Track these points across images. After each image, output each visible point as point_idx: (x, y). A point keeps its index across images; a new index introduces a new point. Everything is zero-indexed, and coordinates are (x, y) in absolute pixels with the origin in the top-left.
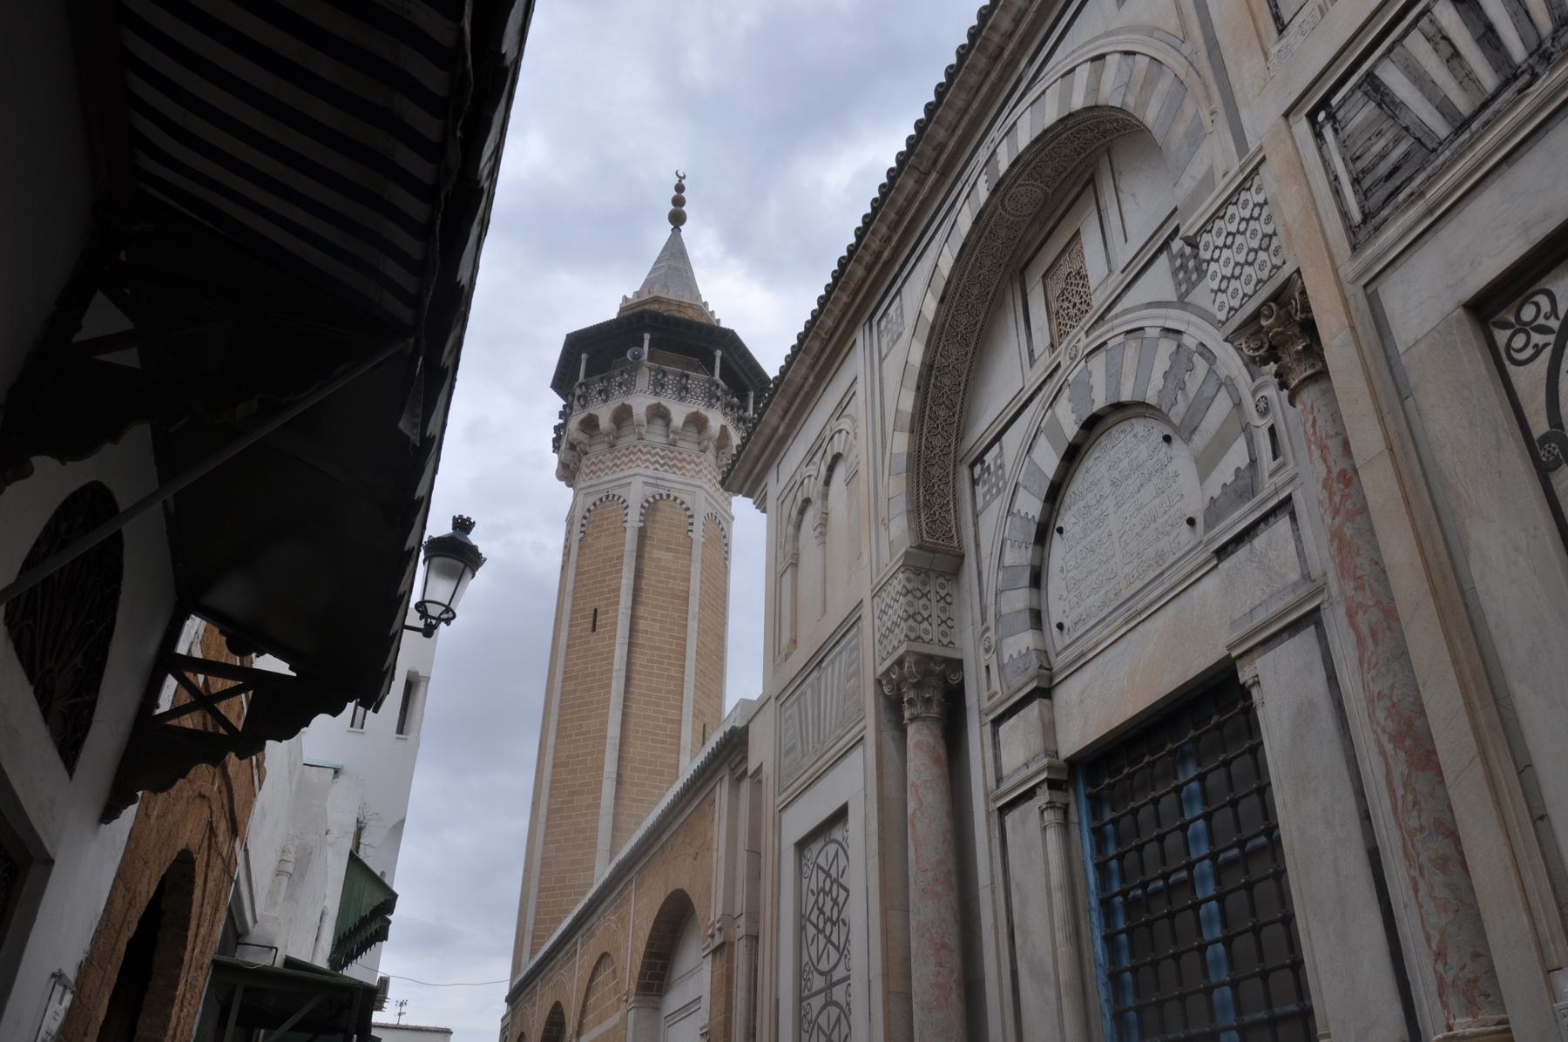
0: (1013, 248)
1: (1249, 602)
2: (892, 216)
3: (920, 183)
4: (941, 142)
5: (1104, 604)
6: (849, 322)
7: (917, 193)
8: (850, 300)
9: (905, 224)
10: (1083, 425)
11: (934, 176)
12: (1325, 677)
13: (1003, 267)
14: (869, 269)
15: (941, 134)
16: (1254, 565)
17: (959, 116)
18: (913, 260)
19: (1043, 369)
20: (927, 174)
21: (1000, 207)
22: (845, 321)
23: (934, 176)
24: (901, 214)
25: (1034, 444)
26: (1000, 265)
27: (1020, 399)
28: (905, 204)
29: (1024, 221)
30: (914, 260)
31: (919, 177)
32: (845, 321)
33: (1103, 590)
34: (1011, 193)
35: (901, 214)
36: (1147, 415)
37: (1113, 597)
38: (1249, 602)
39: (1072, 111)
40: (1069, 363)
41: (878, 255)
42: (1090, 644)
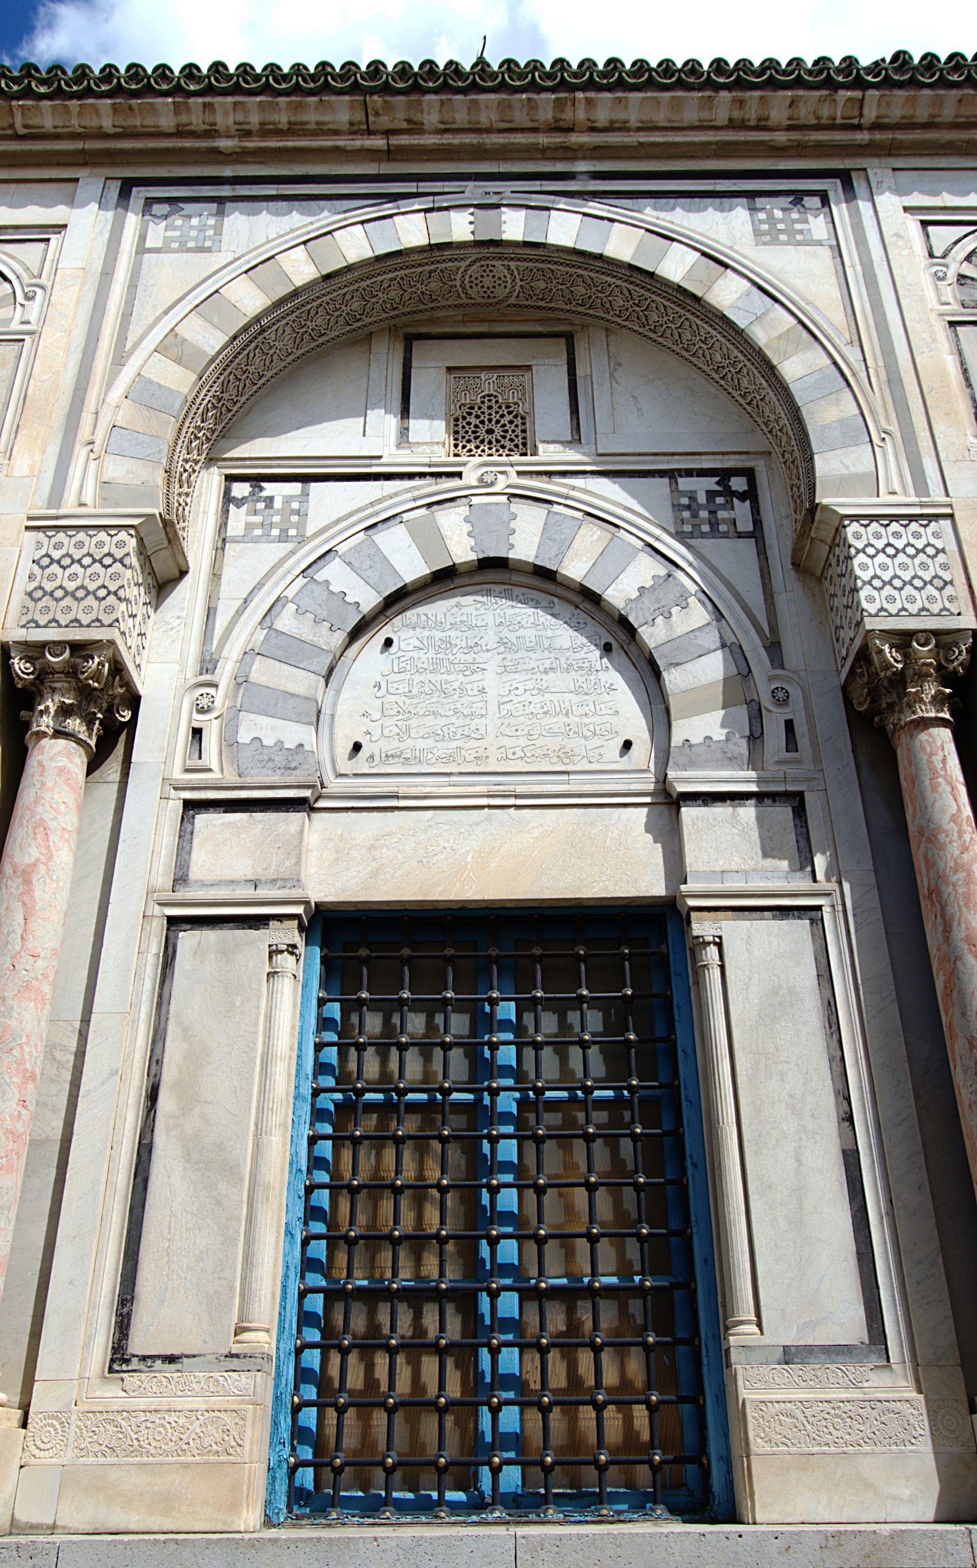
0: (422, 307)
1: (721, 862)
2: (282, 119)
3: (353, 130)
4: (423, 124)
5: (450, 759)
6: (83, 151)
7: (336, 133)
8: (112, 131)
9: (291, 144)
10: (484, 559)
11: (379, 142)
12: (814, 972)
13: (396, 312)
14: (180, 133)
15: (431, 118)
16: (735, 831)
17: (467, 126)
18: (271, 190)
19: (427, 460)
20: (370, 132)
21: (468, 262)
22: (79, 145)
23: (379, 142)
24: (294, 130)
25: (380, 526)
26: (395, 309)
27: (370, 466)
28: (313, 127)
29: (459, 296)
30: (274, 193)
31: (360, 123)
32: (79, 145)
33: (453, 745)
34: (494, 263)
35: (294, 130)
36: (581, 606)
37: (471, 758)
38: (721, 862)
39: (657, 272)
40: (475, 483)
41: (211, 133)
42: (413, 791)
